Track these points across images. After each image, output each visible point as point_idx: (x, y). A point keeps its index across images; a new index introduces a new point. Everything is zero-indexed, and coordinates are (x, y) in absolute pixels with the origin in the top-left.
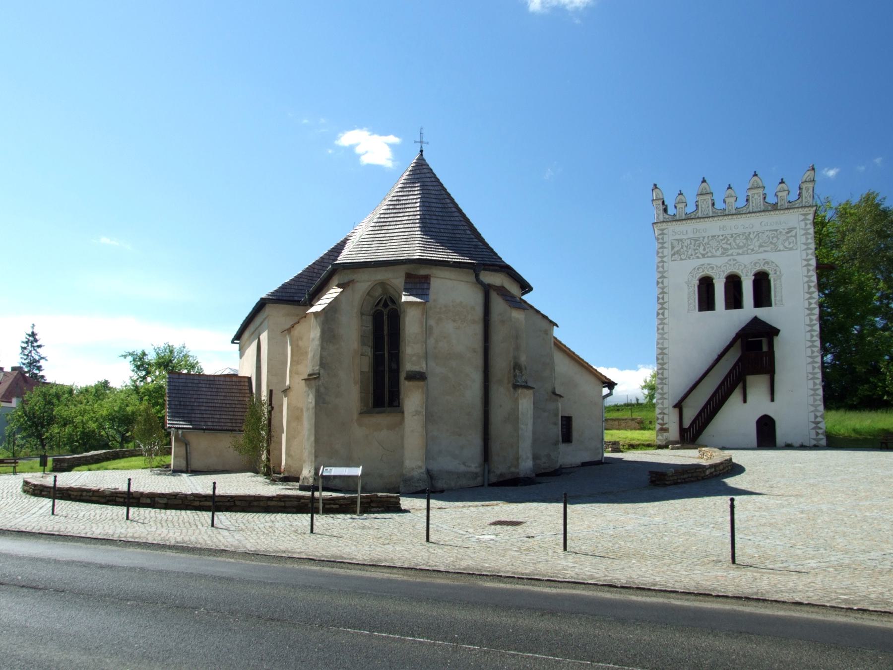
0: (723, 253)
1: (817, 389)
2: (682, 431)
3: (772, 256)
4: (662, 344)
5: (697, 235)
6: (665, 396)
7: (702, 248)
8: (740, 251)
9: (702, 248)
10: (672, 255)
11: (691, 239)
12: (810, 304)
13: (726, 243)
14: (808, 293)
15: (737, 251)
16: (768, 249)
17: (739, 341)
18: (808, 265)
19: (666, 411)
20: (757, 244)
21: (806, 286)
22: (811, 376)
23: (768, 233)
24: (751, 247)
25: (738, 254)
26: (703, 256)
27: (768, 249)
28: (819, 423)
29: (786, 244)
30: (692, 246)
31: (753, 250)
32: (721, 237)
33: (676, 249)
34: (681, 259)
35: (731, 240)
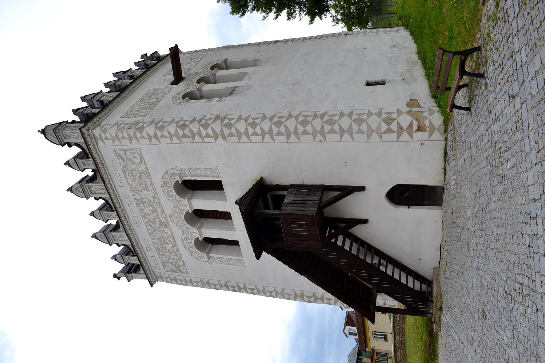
0: (166, 226)
3: (157, 178)
5: (154, 249)
7: (165, 245)
9: (165, 245)
10: (181, 272)
16: (147, 180)
21: (184, 140)
22: (319, 137)
23: (130, 181)
25: (163, 212)
28: (400, 127)
29: (137, 161)
32: (149, 227)
33: (174, 268)
34: (184, 265)
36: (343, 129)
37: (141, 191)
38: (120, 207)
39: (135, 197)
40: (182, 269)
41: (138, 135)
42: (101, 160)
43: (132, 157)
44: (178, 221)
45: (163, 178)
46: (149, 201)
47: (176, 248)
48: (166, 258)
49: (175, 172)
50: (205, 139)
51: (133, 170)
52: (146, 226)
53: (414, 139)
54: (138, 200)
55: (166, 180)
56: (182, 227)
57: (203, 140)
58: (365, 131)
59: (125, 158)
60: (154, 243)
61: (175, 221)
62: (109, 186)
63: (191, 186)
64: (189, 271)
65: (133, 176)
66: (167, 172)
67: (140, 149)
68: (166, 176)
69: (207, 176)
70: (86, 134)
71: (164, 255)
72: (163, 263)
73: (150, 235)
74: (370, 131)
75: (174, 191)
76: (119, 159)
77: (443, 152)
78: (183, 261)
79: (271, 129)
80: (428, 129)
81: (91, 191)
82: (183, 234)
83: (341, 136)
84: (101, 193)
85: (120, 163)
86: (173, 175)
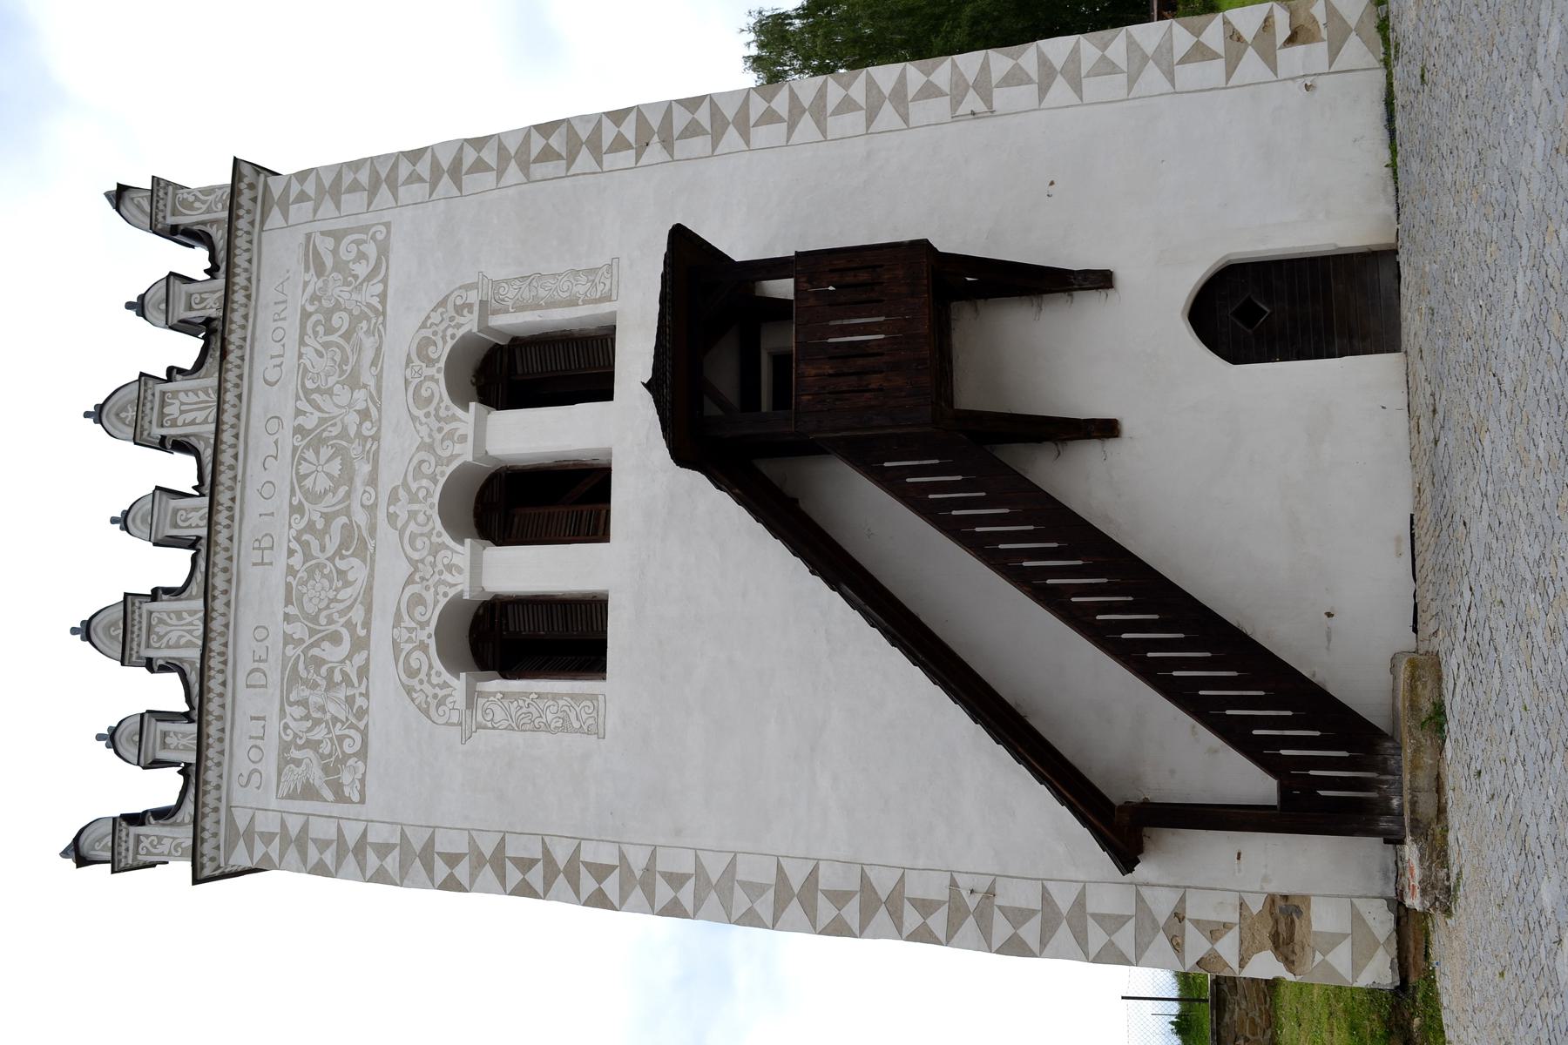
1: (1044, 62)
2: (1300, 811)
3: (402, 331)
5: (275, 677)
6: (1064, 901)
8: (364, 469)
10: (341, 798)
11: (285, 701)
13: (321, 535)
14: (571, 159)
15: (358, 482)
16: (369, 343)
17: (771, 468)
19: (1162, 904)
20: (342, 395)
22: (972, 102)
24: (352, 419)
25: (373, 480)
26: (361, 644)
27: (369, 343)
29: (361, 270)
30: (315, 698)
31: (365, 415)
32: (296, 561)
34: (363, 754)
35: (314, 513)
36: (1051, 67)
37: (329, 392)
38: (232, 468)
39: (301, 420)
40: (346, 778)
42: (249, 280)
43: (353, 256)
44: (412, 515)
45: (423, 326)
46: (344, 434)
47: (359, 659)
48: (307, 717)
51: (338, 307)
52: (291, 553)
53: (1282, 73)
55: (427, 333)
56: (419, 544)
57: (600, 163)
60: (288, 639)
61: (403, 516)
62: (231, 376)
64: (370, 791)
66: (443, 303)
67: (388, 225)
68: (436, 318)
70: (246, 180)
71: (303, 703)
72: (285, 747)
73: (288, 601)
75: (441, 377)
76: (307, 269)
77: (1380, 109)
78: (364, 734)
80: (1324, 33)
81: (162, 415)
82: (410, 581)
83: (1043, 90)
84: (193, 423)
85: (306, 284)
86: (459, 310)
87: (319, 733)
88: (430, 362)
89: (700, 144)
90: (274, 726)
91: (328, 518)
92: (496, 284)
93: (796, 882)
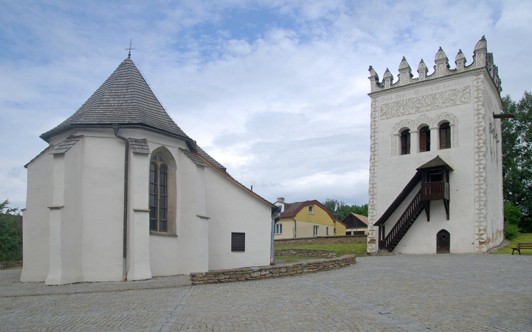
0: (416, 111)
3: (451, 110)
4: (373, 180)
5: (398, 100)
7: (402, 108)
9: (402, 108)
10: (382, 116)
12: (479, 144)
13: (419, 103)
15: (426, 108)
16: (450, 104)
18: (479, 114)
20: (441, 101)
21: (476, 130)
22: (477, 199)
25: (427, 110)
26: (403, 114)
29: (463, 99)
31: (438, 106)
32: (415, 99)
33: (384, 111)
34: (388, 118)
40: (384, 116)
41: (480, 103)
44: (421, 119)
46: (435, 103)
47: (401, 115)
49: (456, 122)
50: (477, 142)
51: (456, 96)
54: (435, 96)
58: (480, 220)
59: (465, 92)
60: (403, 101)
61: (421, 117)
62: (445, 78)
63: (445, 128)
64: (383, 121)
65: (452, 95)
66: (455, 117)
68: (453, 116)
69: (453, 140)
72: (388, 104)
73: (409, 99)
74: (480, 222)
79: (482, 176)
86: (454, 120)
87: (390, 110)
88: (445, 117)
89: (477, 157)
90: (390, 101)
91: (421, 104)
92: (457, 126)
93: (375, 186)
